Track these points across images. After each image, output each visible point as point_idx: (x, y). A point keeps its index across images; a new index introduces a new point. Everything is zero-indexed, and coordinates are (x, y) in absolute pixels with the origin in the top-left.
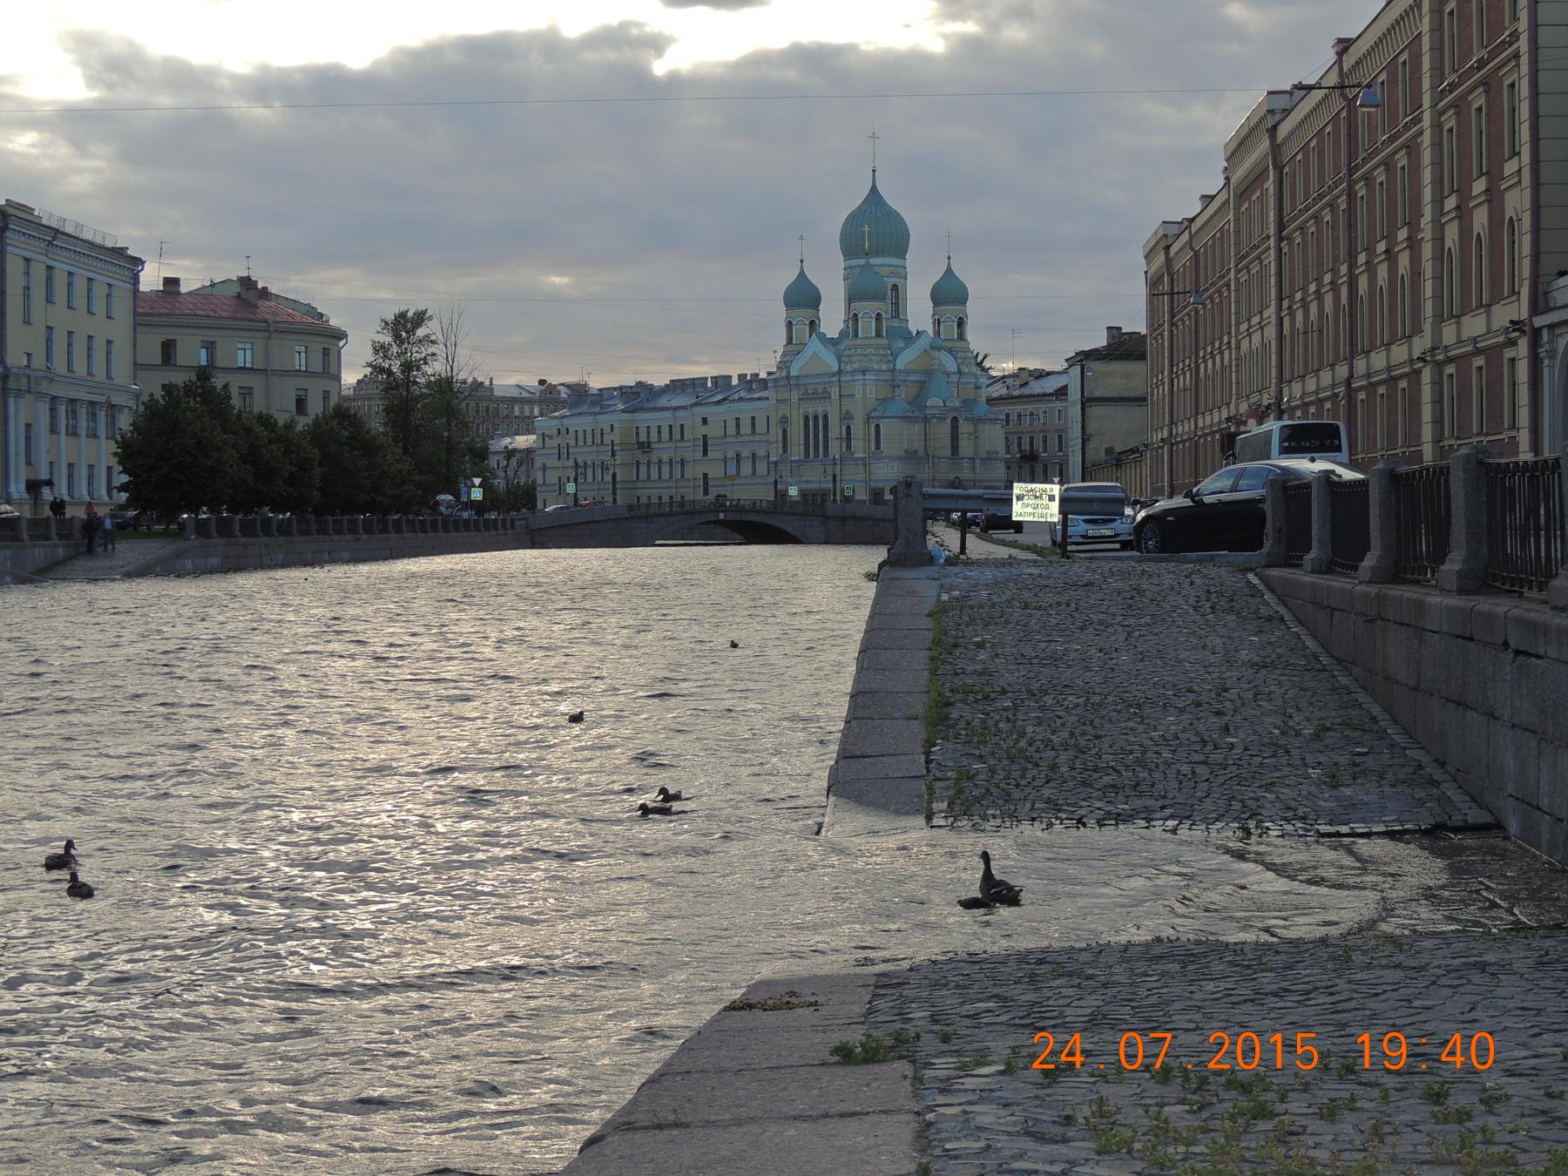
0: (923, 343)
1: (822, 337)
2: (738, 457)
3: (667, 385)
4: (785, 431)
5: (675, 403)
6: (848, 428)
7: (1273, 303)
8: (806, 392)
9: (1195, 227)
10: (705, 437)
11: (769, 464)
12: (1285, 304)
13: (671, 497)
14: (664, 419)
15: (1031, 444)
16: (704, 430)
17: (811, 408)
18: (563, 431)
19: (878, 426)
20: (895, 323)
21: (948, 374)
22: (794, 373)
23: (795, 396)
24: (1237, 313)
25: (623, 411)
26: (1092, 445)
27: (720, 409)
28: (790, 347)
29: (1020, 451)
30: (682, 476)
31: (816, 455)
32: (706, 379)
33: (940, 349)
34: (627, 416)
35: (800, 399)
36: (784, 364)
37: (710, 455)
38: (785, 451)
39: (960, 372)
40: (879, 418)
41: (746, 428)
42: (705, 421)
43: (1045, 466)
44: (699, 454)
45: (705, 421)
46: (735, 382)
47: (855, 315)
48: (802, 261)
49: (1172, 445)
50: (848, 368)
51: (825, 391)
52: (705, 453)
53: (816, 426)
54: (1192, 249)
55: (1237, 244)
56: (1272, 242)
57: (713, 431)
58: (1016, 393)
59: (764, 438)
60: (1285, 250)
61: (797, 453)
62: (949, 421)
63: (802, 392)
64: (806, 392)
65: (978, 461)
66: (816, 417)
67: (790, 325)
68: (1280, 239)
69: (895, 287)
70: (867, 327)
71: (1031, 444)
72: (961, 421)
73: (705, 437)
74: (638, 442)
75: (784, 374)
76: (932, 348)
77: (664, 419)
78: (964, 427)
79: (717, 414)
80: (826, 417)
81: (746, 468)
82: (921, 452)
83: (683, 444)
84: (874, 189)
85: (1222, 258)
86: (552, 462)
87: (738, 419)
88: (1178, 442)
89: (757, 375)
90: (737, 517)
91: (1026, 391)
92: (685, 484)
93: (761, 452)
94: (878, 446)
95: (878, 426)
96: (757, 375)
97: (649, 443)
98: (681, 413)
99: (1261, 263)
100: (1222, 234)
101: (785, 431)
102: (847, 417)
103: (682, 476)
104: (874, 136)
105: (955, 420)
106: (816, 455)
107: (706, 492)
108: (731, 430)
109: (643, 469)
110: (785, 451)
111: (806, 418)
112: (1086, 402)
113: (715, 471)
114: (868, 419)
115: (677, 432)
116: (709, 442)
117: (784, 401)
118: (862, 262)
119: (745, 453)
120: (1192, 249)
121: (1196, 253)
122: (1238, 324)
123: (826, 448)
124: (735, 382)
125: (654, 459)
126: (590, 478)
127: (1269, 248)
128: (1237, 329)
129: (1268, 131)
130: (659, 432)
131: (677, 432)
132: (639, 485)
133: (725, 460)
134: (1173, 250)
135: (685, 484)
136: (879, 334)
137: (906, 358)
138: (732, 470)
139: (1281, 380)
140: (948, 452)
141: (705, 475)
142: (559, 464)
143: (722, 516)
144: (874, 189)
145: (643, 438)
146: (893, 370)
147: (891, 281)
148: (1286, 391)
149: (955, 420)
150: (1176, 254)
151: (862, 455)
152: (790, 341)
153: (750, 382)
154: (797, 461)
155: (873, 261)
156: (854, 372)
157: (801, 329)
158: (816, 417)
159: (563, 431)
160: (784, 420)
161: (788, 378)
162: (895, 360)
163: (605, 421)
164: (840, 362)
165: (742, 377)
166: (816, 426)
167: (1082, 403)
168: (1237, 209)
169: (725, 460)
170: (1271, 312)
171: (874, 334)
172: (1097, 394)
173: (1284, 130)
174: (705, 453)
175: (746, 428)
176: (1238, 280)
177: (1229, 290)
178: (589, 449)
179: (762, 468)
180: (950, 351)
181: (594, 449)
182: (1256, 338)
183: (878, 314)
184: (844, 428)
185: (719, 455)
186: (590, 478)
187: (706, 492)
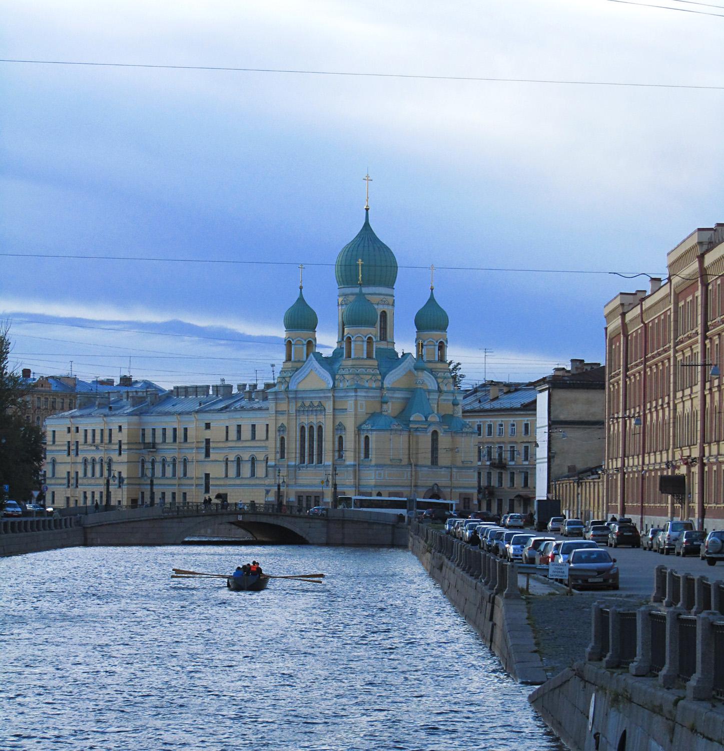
0: (407, 365)
1: (318, 356)
2: (239, 460)
3: (172, 391)
4: (282, 439)
6: (341, 438)
7: (699, 383)
8: (303, 405)
9: (647, 304)
10: (208, 441)
11: (267, 467)
12: (708, 385)
13: (174, 494)
14: (170, 423)
15: (500, 455)
16: (208, 434)
17: (306, 420)
18: (73, 429)
19: (367, 438)
20: (383, 345)
21: (429, 391)
22: (292, 387)
23: (293, 408)
24: (675, 383)
25: (129, 414)
26: (556, 461)
27: (224, 416)
28: (289, 364)
29: (490, 459)
30: (185, 474)
32: (208, 387)
33: (423, 369)
34: (135, 419)
35: (297, 411)
36: (283, 380)
37: (213, 456)
38: (282, 457)
39: (440, 391)
40: (367, 430)
41: (246, 434)
43: (513, 474)
44: (202, 456)
45: (208, 426)
47: (349, 338)
48: (301, 288)
49: (624, 473)
50: (341, 385)
51: (320, 404)
52: (207, 455)
54: (643, 322)
55: (676, 330)
56: (699, 337)
57: (216, 434)
58: (487, 406)
59: (263, 444)
60: (708, 346)
61: (293, 459)
62: (430, 434)
64: (303, 405)
65: (454, 470)
66: (311, 428)
67: (289, 344)
68: (705, 337)
69: (384, 314)
70: (359, 349)
71: (500, 455)
72: (441, 434)
74: (144, 443)
75: (283, 387)
76: (416, 369)
77: (170, 423)
78: (444, 441)
79: (220, 422)
80: (320, 428)
81: (246, 470)
83: (187, 445)
84: (367, 225)
85: (665, 335)
86: (62, 457)
87: (239, 426)
88: (630, 472)
89: (255, 386)
90: (252, 519)
91: (496, 405)
92: (189, 482)
93: (260, 457)
94: (367, 455)
96: (255, 386)
97: (154, 445)
99: (692, 350)
100: (665, 316)
101: (282, 439)
102: (339, 428)
103: (185, 474)
104: (368, 179)
105: (435, 433)
108: (233, 435)
109: (148, 466)
110: (282, 457)
111: (303, 428)
112: (553, 424)
113: (216, 471)
114: (359, 429)
115: (180, 434)
116: (212, 445)
117: (282, 413)
118: (357, 290)
119: (246, 456)
120: (643, 322)
121: (646, 325)
122: (675, 392)
123: (320, 454)
124: (235, 391)
125: (158, 459)
126: (98, 474)
127: (697, 342)
128: (675, 397)
129: (698, 257)
130: (164, 434)
131: (180, 434)
134: (629, 317)
135: (189, 482)
136: (369, 357)
137: (393, 378)
138: (232, 472)
139: (703, 441)
140: (429, 463)
141: (207, 476)
142: (68, 459)
143: (240, 518)
144: (367, 225)
145: (149, 439)
146: (382, 388)
147: (380, 309)
148: (707, 449)
149: (435, 433)
150: (631, 321)
151: (352, 463)
152: (289, 359)
153: (250, 392)
155: (365, 290)
156: (346, 390)
157: (299, 351)
158: (311, 428)
159: (73, 429)
160: (282, 429)
162: (383, 378)
163: (114, 422)
164: (334, 379)
165: (242, 387)
167: (549, 426)
168: (676, 304)
170: (697, 388)
171: (365, 356)
172: (562, 417)
173: (709, 259)
174: (207, 455)
175: (246, 434)
176: (675, 358)
177: (669, 362)
179: (260, 471)
180: (431, 371)
182: (688, 404)
183: (370, 338)
184: (337, 439)
185: (221, 457)
186: (98, 474)
187: (207, 490)
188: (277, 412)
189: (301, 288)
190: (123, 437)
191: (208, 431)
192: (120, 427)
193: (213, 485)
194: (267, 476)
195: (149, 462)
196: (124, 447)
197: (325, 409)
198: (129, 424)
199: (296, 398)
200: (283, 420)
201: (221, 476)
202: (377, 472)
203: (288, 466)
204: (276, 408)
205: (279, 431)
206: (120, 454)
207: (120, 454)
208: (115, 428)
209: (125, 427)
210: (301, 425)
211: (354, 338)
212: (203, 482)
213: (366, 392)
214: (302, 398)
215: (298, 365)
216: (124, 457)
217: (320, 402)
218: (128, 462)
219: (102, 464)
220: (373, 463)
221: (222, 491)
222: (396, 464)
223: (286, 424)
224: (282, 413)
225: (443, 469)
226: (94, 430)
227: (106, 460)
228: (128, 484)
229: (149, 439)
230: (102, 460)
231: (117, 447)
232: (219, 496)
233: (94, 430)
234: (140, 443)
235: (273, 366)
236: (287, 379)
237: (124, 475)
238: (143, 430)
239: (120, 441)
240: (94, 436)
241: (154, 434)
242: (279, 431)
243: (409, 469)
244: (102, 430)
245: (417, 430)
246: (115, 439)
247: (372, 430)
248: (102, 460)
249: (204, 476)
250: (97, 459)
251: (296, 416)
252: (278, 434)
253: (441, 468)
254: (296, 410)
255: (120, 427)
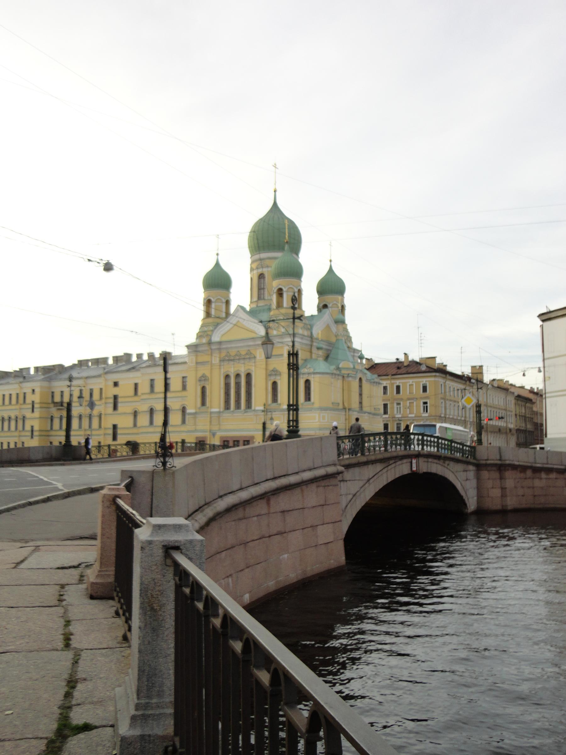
4: (203, 389)
5: (85, 374)
6: (275, 384)
10: (115, 397)
16: (116, 391)
17: (232, 370)
22: (216, 338)
28: (210, 320)
30: (90, 426)
31: (238, 406)
35: (222, 360)
38: (203, 403)
40: (309, 374)
42: (116, 384)
46: (134, 359)
48: (217, 254)
51: (249, 353)
52: (115, 408)
53: (238, 385)
63: (223, 354)
66: (238, 376)
73: (115, 397)
74: (53, 402)
80: (249, 376)
82: (341, 406)
84: (275, 204)
95: (307, 382)
98: (90, 381)
101: (203, 389)
103: (90, 426)
106: (238, 406)
107: (115, 438)
110: (203, 403)
111: (227, 377)
116: (120, 400)
117: (203, 363)
131: (86, 395)
132: (53, 433)
133: (135, 414)
141: (115, 427)
144: (275, 204)
145: (57, 399)
146: (311, 337)
152: (208, 314)
154: (219, 412)
158: (238, 376)
161: (210, 343)
164: (265, 327)
166: (238, 385)
169: (135, 414)
174: (115, 408)
178: (13, 407)
181: (17, 407)
187: (115, 438)
188: (197, 363)
189: (217, 254)
190: (37, 398)
191: (116, 388)
192: (33, 390)
193: (121, 434)
194: (184, 422)
195: (57, 418)
196: (36, 406)
197: (255, 357)
198: (41, 387)
199: (219, 349)
200: (204, 370)
201: (144, 425)
202: (322, 415)
203: (211, 413)
204: (196, 359)
205: (200, 380)
206: (33, 411)
207: (33, 411)
208: (29, 391)
209: (37, 390)
210: (226, 374)
211: (286, 288)
212: (111, 432)
213: (302, 338)
214: (227, 348)
215: (218, 321)
216: (37, 414)
217: (249, 350)
218: (40, 418)
219: (17, 421)
220: (317, 405)
221: (132, 438)
222: (334, 408)
223: (208, 374)
224: (203, 363)
225: (366, 414)
226: (10, 395)
227: (20, 417)
228: (40, 436)
229: (57, 399)
230: (17, 417)
231: (30, 406)
232: (128, 443)
233: (10, 395)
234: (49, 403)
235: (173, 334)
236: (209, 333)
237: (36, 428)
238: (53, 393)
239: (33, 402)
240: (10, 398)
241: (62, 396)
242: (200, 380)
243: (344, 413)
244: (17, 394)
245: (348, 376)
246: (29, 401)
247: (314, 373)
248: (17, 417)
249: (111, 427)
250: (13, 417)
251: (220, 366)
252: (198, 383)
253: (365, 413)
254: (220, 361)
255: (33, 390)
